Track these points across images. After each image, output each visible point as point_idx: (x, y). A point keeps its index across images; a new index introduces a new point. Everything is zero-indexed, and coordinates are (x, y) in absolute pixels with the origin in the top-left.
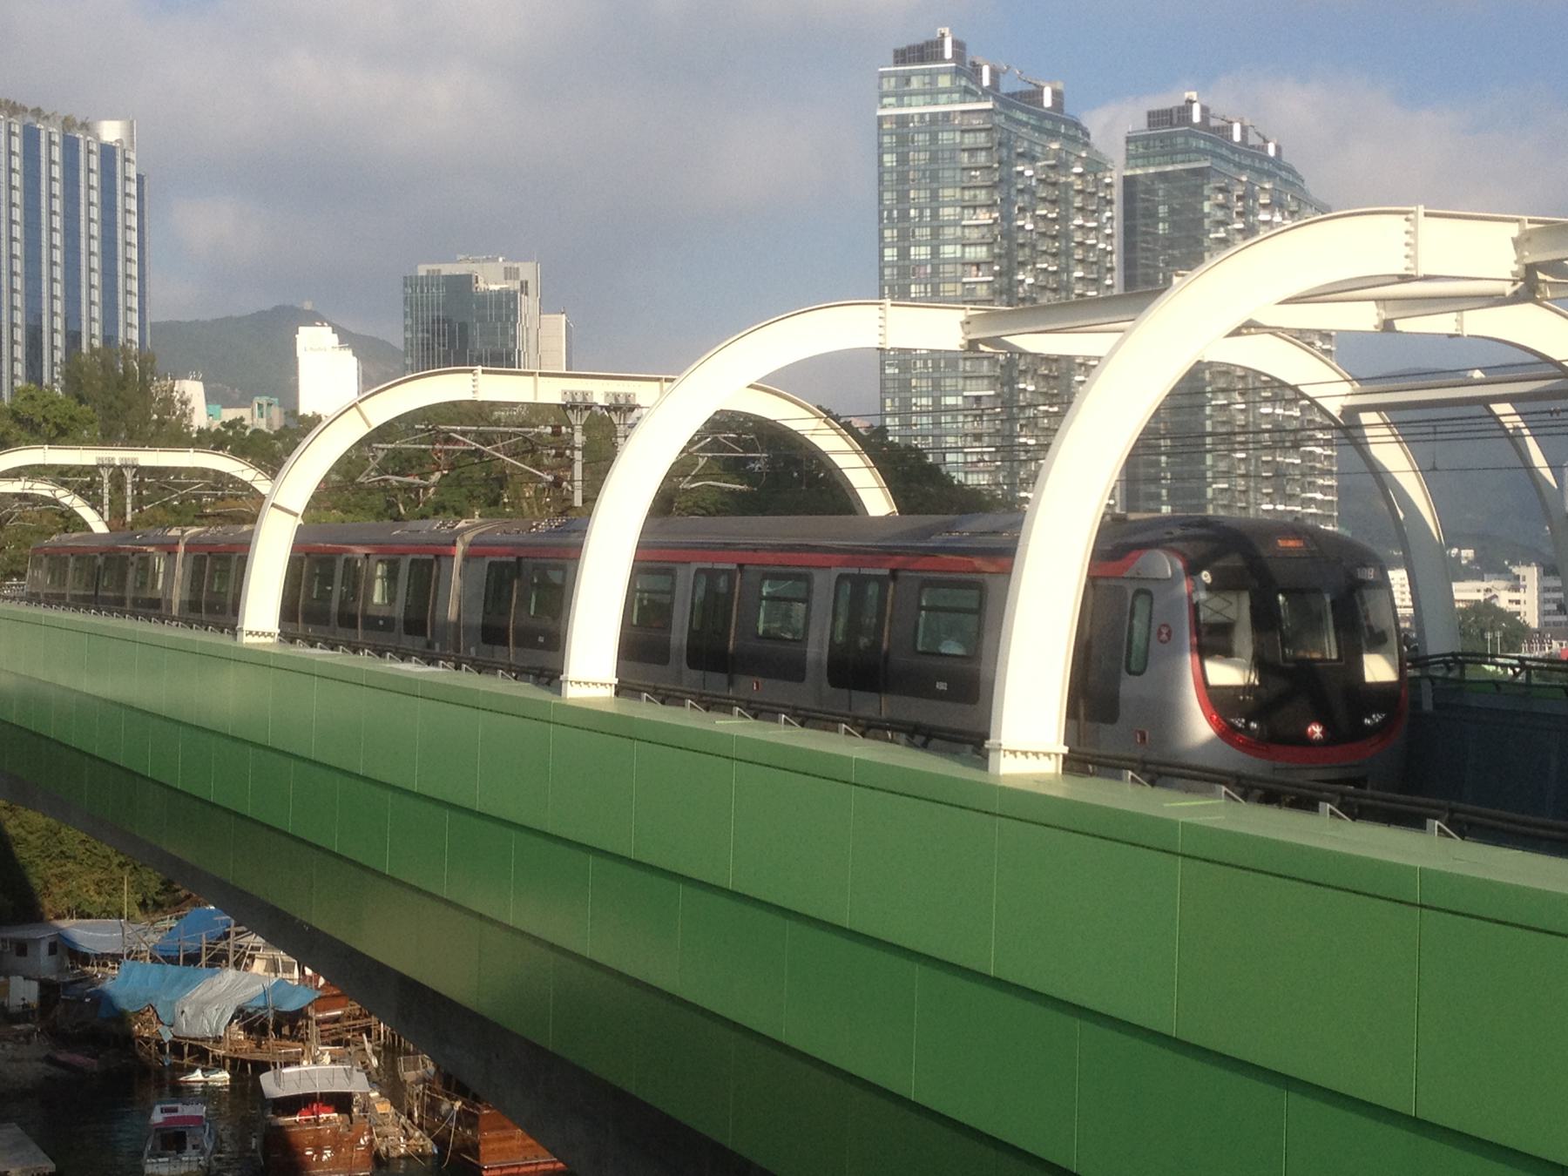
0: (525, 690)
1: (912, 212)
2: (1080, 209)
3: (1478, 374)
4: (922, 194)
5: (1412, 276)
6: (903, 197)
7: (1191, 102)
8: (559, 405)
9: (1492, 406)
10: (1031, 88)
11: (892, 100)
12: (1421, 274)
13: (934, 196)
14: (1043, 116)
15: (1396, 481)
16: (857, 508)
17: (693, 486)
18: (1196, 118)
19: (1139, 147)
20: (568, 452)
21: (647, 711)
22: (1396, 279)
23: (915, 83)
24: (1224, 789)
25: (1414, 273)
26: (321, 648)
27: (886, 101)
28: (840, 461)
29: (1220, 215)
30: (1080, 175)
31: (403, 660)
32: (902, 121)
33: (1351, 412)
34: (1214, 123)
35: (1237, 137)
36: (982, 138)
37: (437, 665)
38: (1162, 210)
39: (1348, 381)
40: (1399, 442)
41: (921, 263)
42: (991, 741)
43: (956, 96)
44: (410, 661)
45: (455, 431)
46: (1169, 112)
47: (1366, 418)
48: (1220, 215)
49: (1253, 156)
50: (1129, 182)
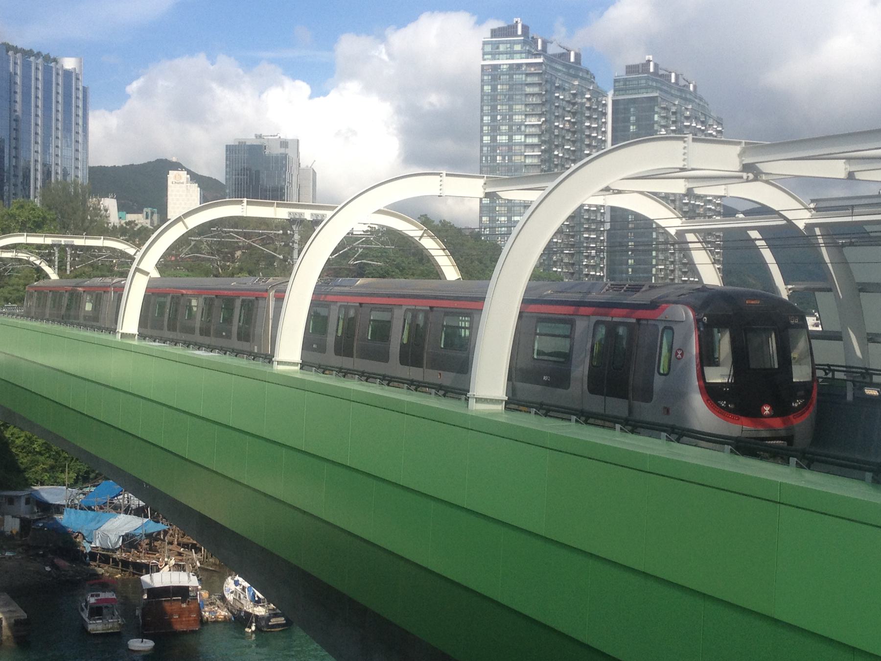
0: (258, 366)
1: (499, 118)
2: (589, 118)
3: (741, 216)
4: (504, 107)
5: (686, 169)
6: (494, 108)
7: (649, 61)
8: (287, 220)
9: (748, 232)
10: (565, 51)
11: (490, 56)
12: (690, 168)
13: (511, 109)
14: (569, 66)
15: (697, 269)
16: (441, 276)
17: (355, 263)
18: (652, 70)
19: (621, 85)
20: (291, 244)
21: (312, 377)
22: (678, 170)
23: (502, 48)
24: (575, 417)
25: (686, 167)
26: (158, 342)
27: (486, 57)
28: (433, 253)
29: (663, 123)
30: (589, 99)
31: (199, 349)
32: (495, 67)
33: (681, 233)
34: (661, 72)
35: (673, 80)
36: (536, 79)
37: (215, 353)
38: (632, 118)
39: (679, 218)
40: (705, 249)
41: (502, 145)
42: (470, 393)
43: (524, 55)
44: (202, 350)
45: (232, 232)
46: (637, 66)
47: (690, 237)
48: (663, 123)
49: (680, 90)
50: (615, 103)
